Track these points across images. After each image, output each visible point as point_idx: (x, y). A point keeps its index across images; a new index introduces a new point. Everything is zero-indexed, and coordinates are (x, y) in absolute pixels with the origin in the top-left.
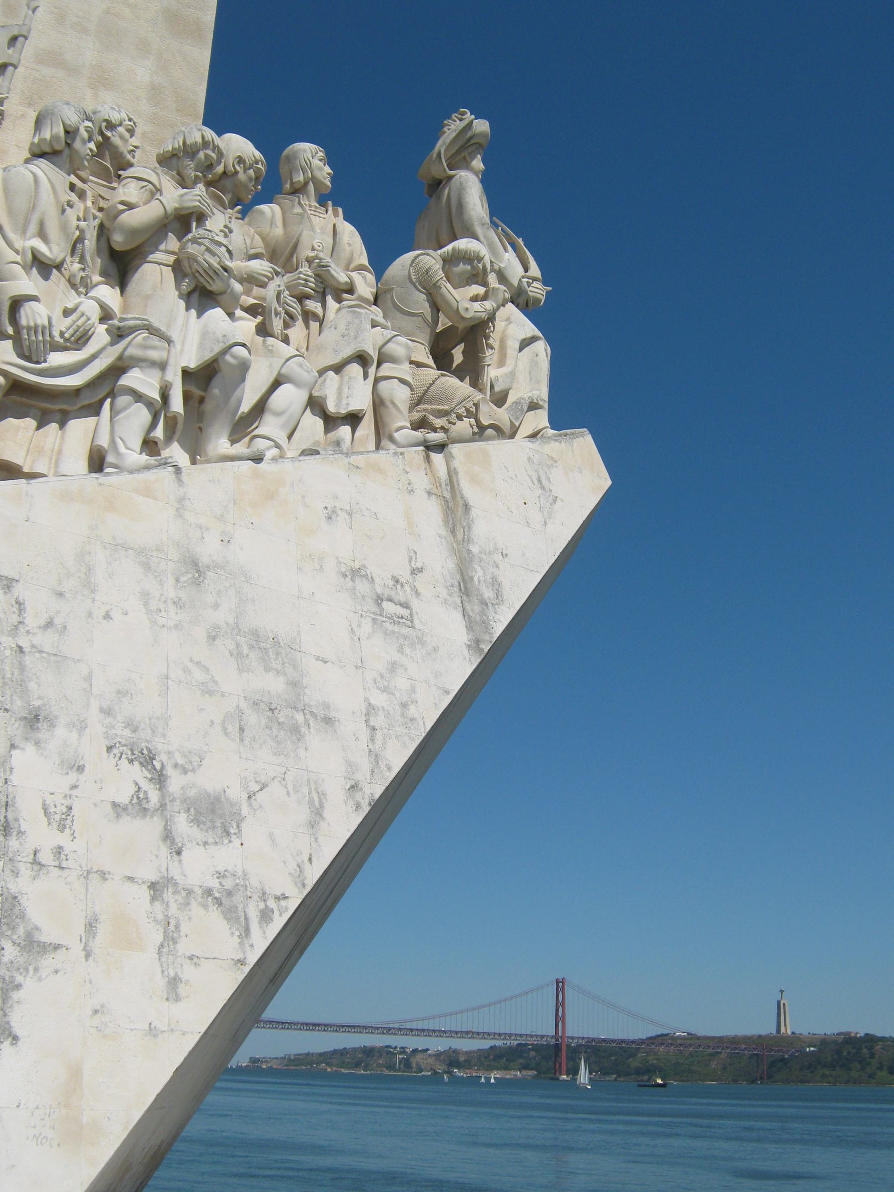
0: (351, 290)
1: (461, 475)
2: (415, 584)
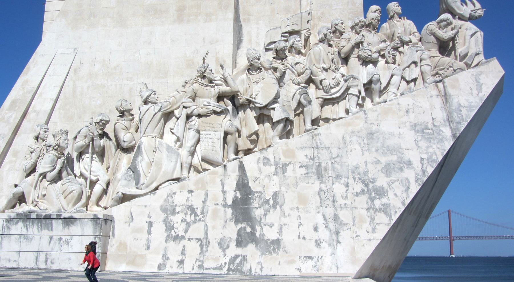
0: (411, 42)
1: (448, 88)
2: (434, 123)
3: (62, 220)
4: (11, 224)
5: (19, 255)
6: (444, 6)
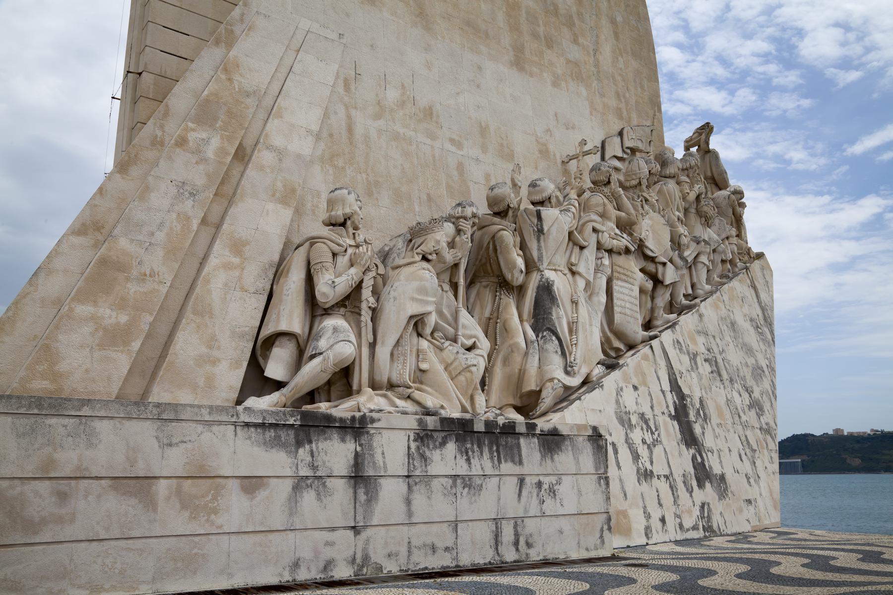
3: (538, 437)
4: (428, 448)
5: (457, 532)
6: (709, 174)
